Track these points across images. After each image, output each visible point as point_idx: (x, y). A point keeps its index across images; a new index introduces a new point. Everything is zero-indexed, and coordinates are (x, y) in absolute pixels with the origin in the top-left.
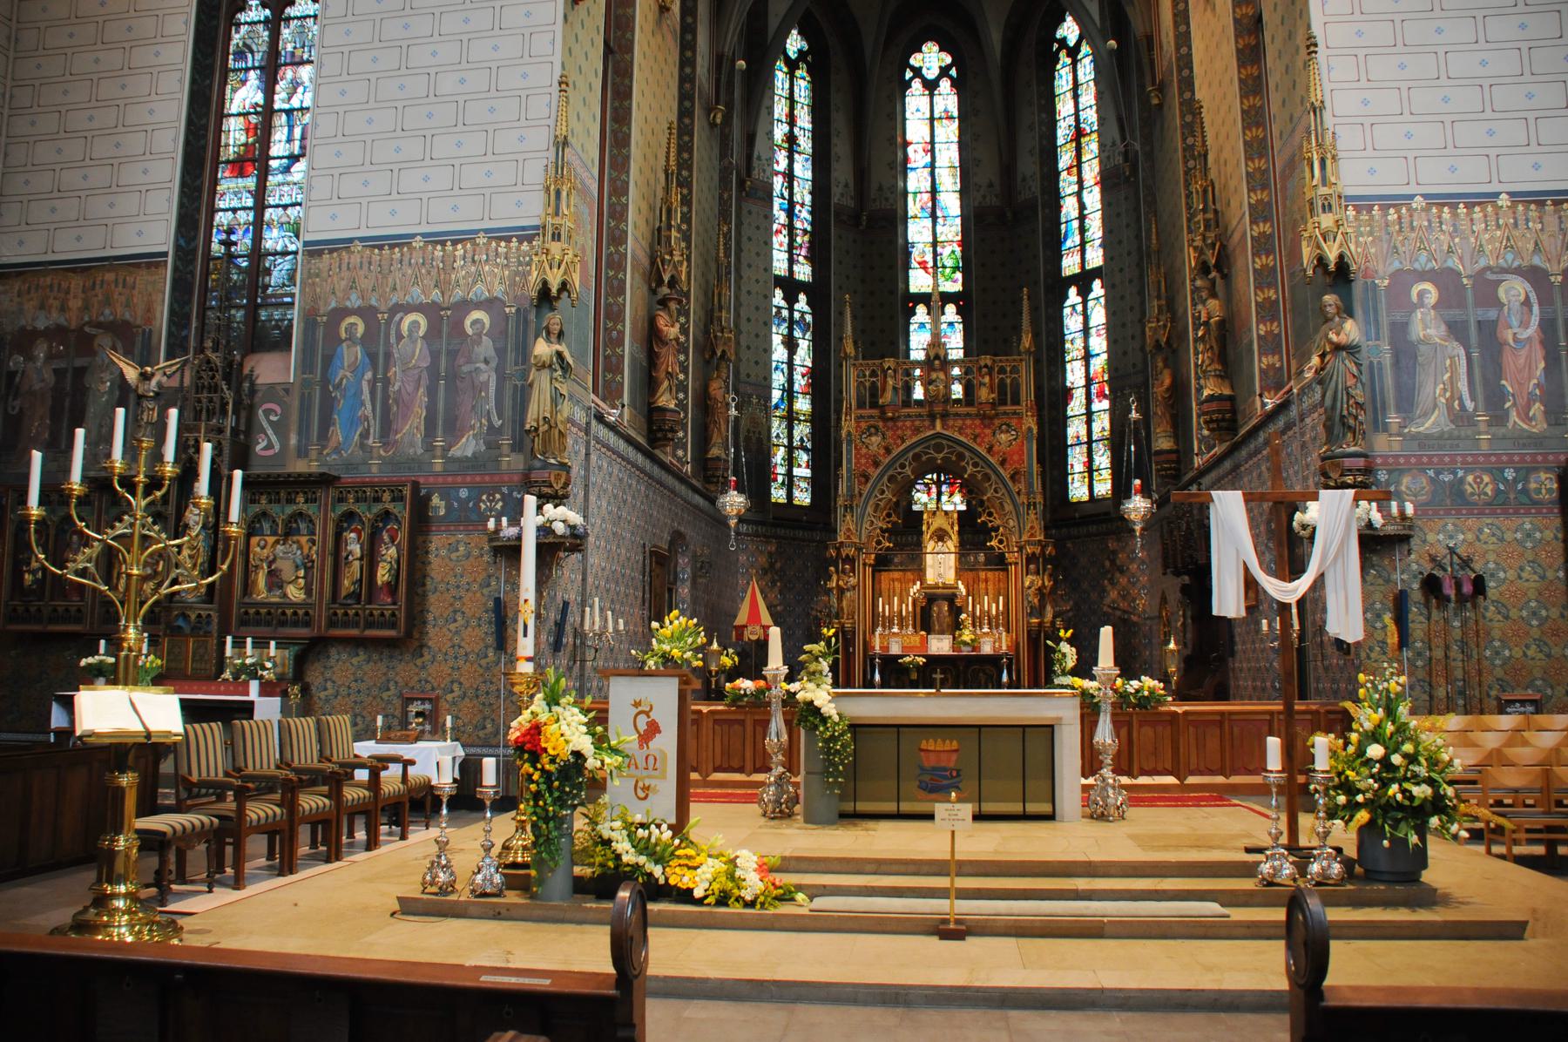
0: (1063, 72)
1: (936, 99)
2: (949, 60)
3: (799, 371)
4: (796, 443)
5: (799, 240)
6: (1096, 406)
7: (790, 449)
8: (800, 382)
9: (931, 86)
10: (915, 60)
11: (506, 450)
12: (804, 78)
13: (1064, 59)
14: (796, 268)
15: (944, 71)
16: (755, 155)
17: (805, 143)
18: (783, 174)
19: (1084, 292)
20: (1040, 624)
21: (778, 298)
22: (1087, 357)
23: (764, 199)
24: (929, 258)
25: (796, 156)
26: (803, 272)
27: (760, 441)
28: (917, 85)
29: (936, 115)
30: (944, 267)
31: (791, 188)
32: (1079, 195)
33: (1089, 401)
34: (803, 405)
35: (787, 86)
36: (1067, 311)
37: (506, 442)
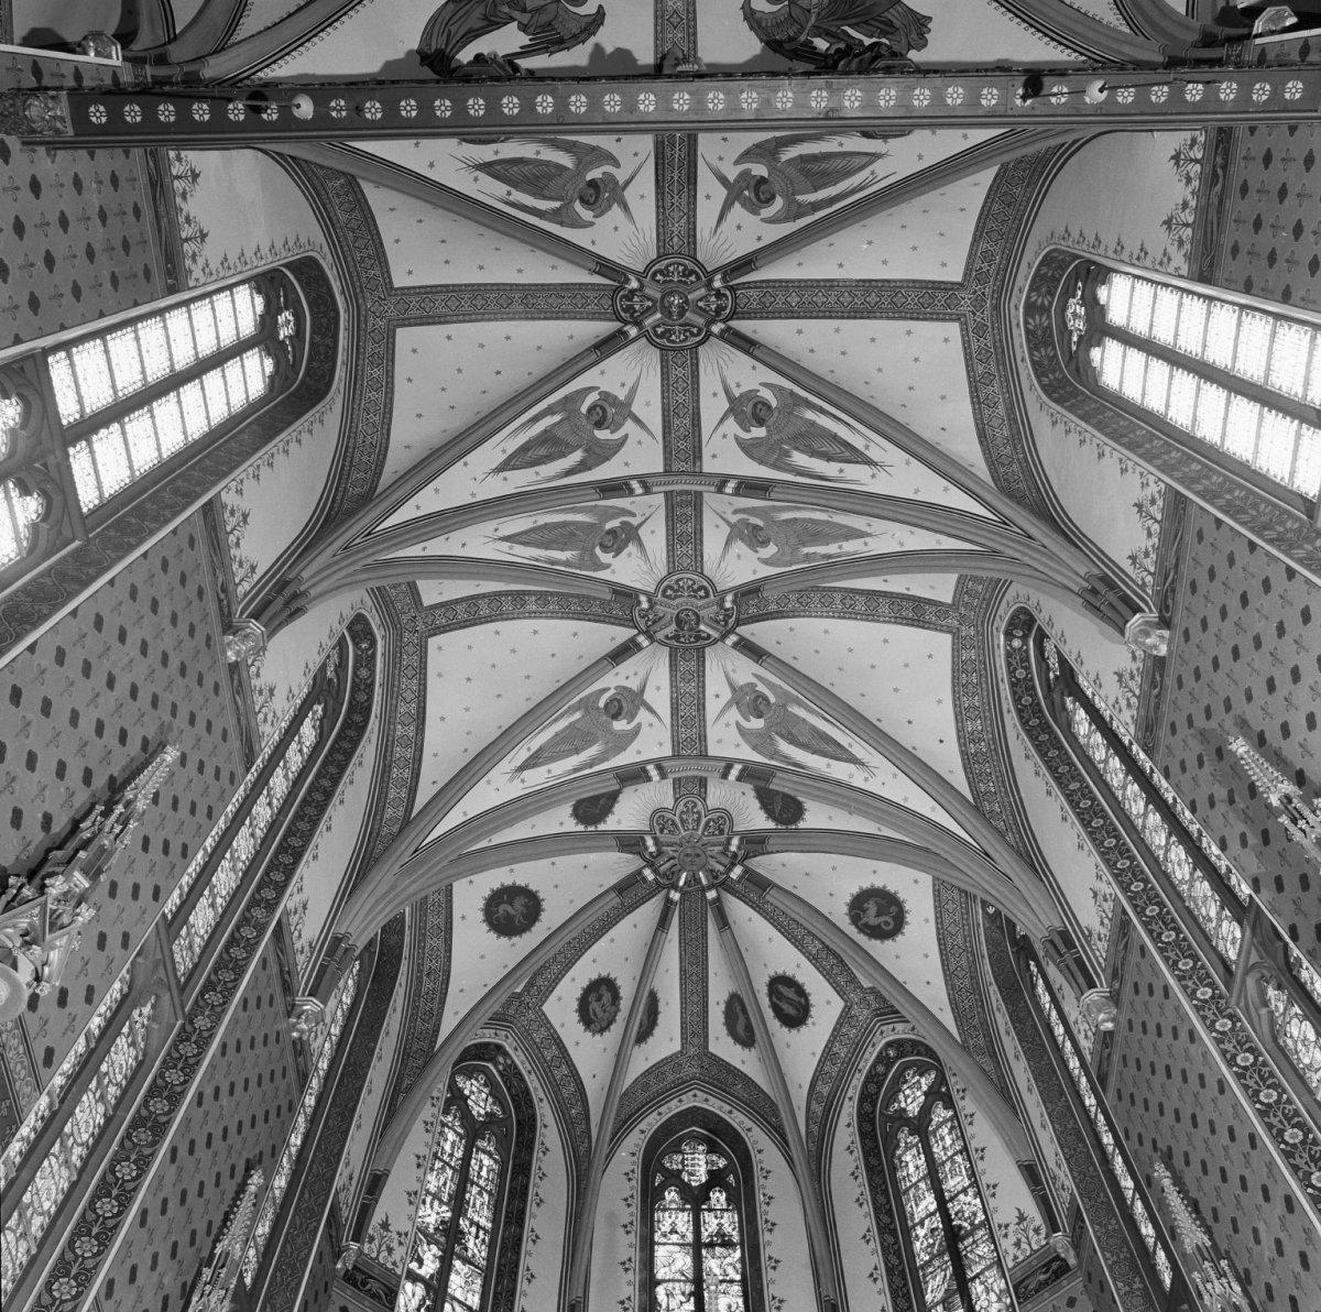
0: (908, 1157)
1: (707, 1217)
2: (722, 1163)
9: (696, 1200)
10: (674, 1162)
12: (489, 1154)
13: (905, 1138)
15: (716, 1179)
16: (377, 1218)
17: (475, 1247)
18: (427, 1283)
23: (374, 1296)
25: (457, 1264)
28: (671, 1195)
29: (705, 1238)
35: (459, 1154)
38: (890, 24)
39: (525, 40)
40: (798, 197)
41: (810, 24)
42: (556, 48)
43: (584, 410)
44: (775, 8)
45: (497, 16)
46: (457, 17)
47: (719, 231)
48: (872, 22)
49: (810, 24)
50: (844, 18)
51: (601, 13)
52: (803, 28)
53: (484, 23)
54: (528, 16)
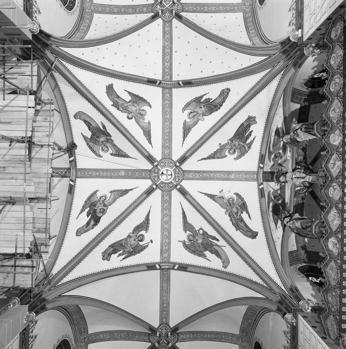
38: (248, 125)
39: (245, 213)
40: (281, 147)
41: (243, 144)
42: (246, 205)
43: (273, 199)
44: (237, 152)
45: (240, 219)
46: (243, 229)
47: (285, 166)
48: (246, 129)
49: (243, 144)
50: (243, 136)
51: (236, 194)
53: (242, 222)
54: (239, 211)
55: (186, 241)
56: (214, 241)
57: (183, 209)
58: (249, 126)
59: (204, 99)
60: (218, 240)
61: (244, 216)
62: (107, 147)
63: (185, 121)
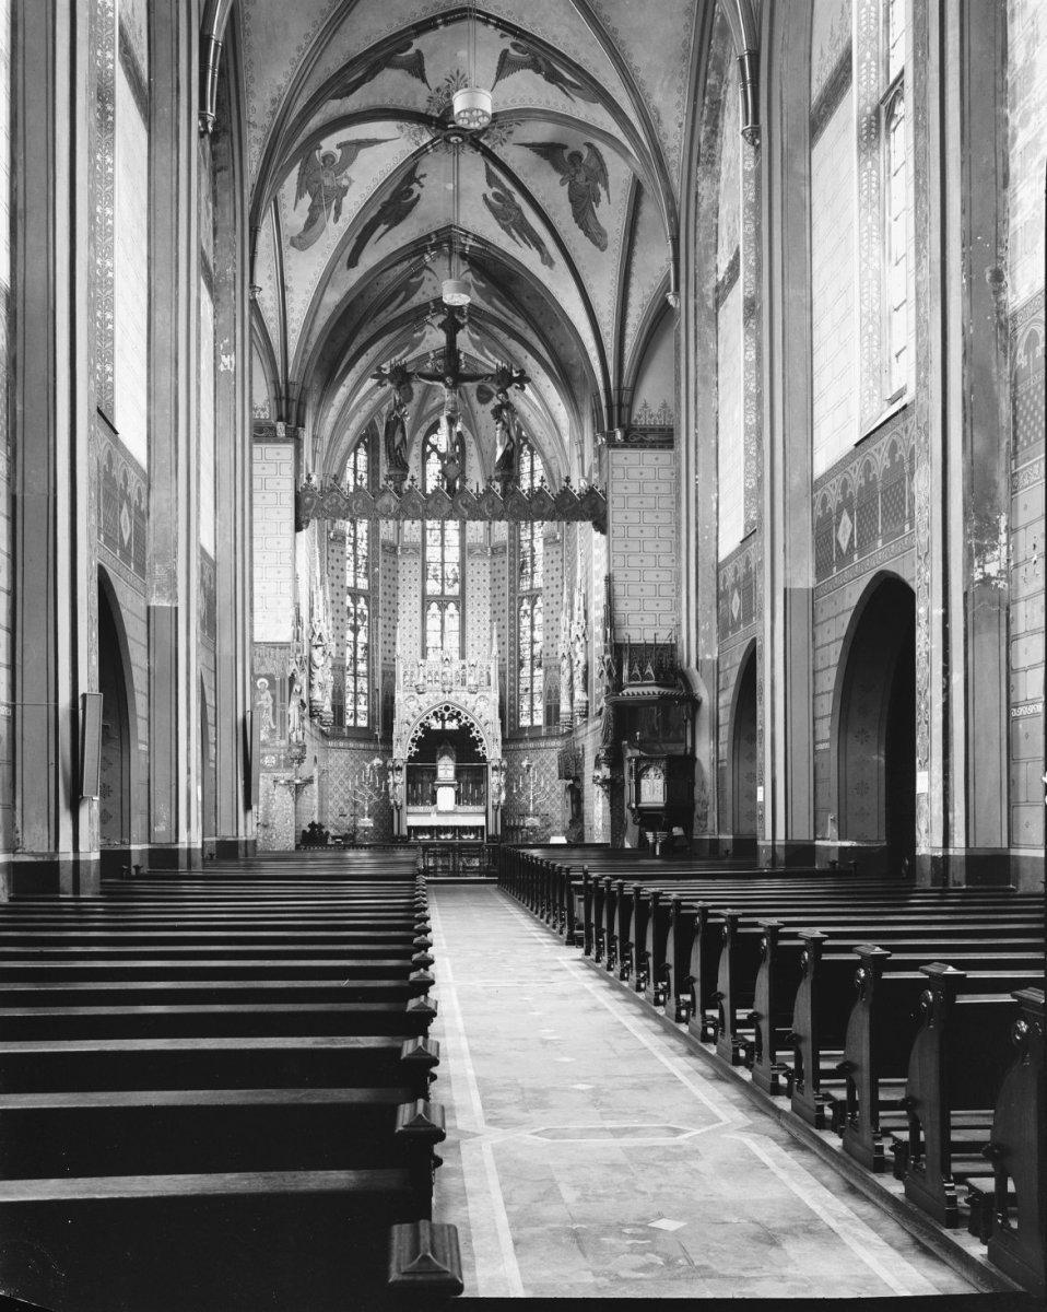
3: (360, 646)
4: (358, 691)
5: (360, 562)
6: (537, 672)
7: (356, 693)
8: (360, 654)
11: (278, 738)
14: (359, 580)
19: (534, 603)
20: (499, 802)
21: (348, 602)
22: (533, 642)
24: (439, 573)
26: (363, 584)
27: (339, 691)
28: (434, 456)
30: (448, 579)
31: (355, 529)
32: (531, 541)
33: (532, 670)
34: (362, 667)
36: (522, 613)
37: (278, 735)
39: (387, 226)
52: (506, 219)
55: (322, 152)
56: (333, 212)
57: (386, 141)
58: (539, 249)
59: (602, 190)
60: (336, 219)
61: (382, 228)
62: (522, 53)
63: (566, 147)
